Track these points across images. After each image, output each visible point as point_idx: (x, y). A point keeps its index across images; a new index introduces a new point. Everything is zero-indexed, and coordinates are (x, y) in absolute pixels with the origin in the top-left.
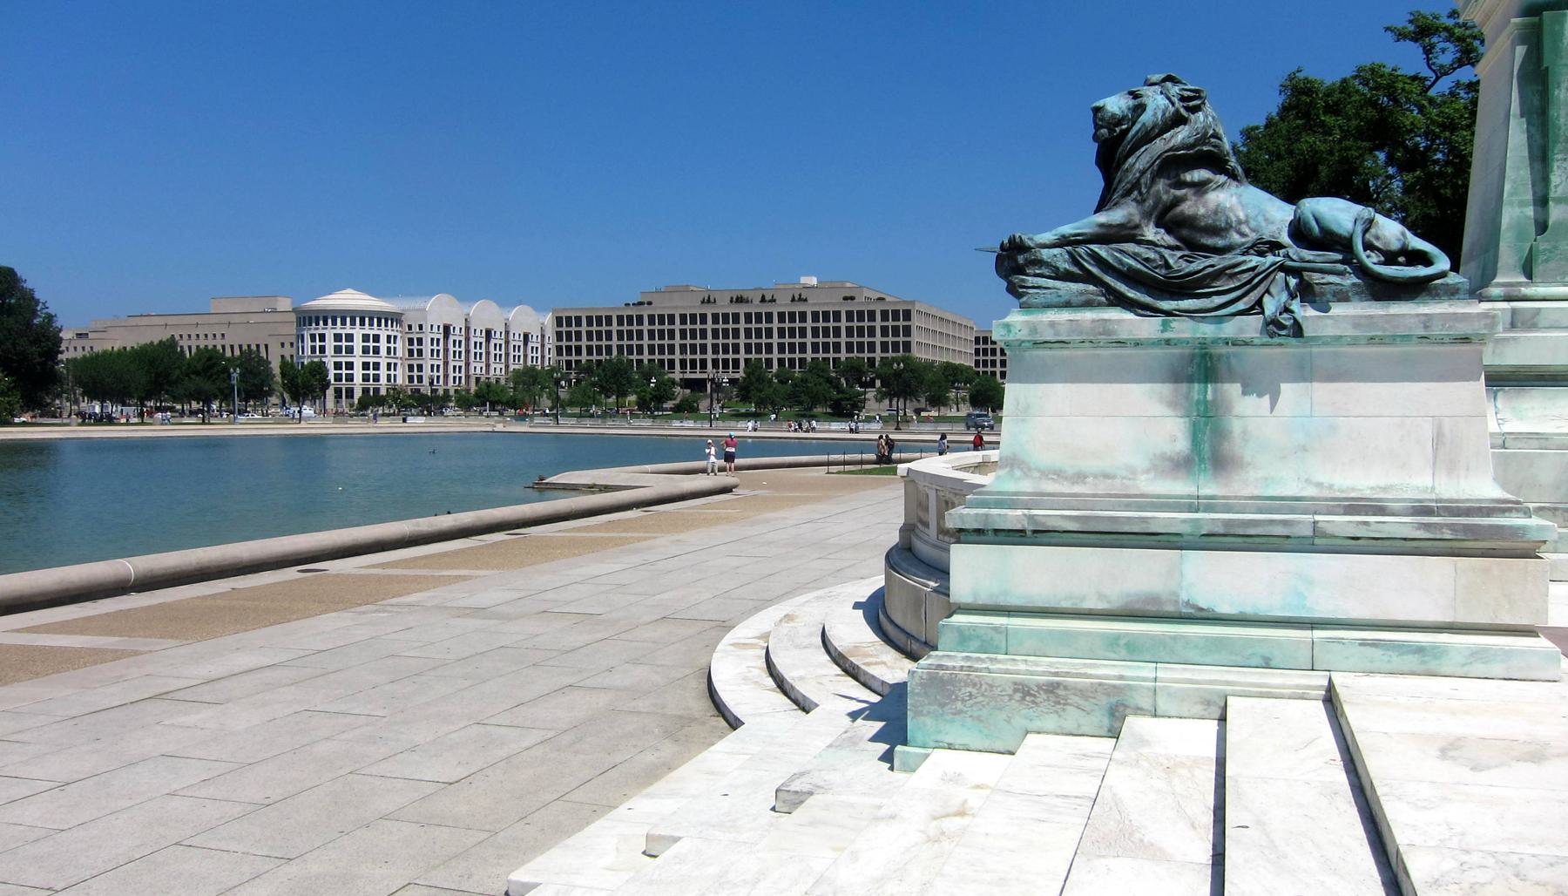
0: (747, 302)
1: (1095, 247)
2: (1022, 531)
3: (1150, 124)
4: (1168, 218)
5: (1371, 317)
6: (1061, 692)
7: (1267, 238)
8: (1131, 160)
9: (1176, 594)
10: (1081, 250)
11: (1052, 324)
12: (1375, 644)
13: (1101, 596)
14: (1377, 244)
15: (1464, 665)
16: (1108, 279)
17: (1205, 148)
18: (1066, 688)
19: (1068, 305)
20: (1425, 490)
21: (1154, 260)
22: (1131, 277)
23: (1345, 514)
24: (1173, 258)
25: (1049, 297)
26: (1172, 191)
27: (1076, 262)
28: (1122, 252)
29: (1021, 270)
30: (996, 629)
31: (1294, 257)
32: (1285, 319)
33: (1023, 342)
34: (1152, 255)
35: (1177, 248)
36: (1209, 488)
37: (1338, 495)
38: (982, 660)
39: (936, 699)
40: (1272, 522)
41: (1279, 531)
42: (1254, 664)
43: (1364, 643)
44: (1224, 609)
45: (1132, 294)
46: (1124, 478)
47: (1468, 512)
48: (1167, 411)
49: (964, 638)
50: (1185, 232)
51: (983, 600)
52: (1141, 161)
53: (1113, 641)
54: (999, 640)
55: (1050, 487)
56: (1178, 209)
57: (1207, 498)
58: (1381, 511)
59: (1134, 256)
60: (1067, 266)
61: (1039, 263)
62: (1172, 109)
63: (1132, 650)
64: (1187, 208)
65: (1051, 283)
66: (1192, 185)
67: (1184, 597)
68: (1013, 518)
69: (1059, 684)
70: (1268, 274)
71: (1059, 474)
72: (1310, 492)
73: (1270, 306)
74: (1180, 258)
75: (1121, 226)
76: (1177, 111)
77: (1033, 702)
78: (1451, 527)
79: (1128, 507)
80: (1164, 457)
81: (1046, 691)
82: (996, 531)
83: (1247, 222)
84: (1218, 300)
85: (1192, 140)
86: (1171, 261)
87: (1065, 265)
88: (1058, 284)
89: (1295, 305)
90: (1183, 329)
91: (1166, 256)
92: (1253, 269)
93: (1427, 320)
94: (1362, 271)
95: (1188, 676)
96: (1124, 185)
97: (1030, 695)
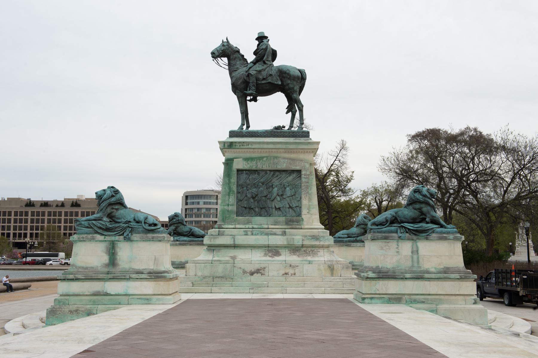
0: (50, 206)
1: (93, 222)
2: (73, 279)
3: (106, 197)
4: (110, 216)
5: (143, 237)
6: (78, 311)
7: (128, 220)
8: (102, 204)
9: (103, 291)
10: (90, 222)
11: (83, 238)
12: (140, 299)
13: (88, 292)
14: (147, 222)
15: (155, 302)
17: (118, 202)
18: (79, 310)
19: (87, 233)
20: (152, 269)
21: (104, 225)
22: (100, 228)
23: (136, 274)
24: (108, 224)
25: (83, 231)
26: (111, 210)
28: (98, 223)
31: (132, 224)
32: (127, 237)
33: (76, 241)
34: (104, 223)
35: (110, 221)
37: (136, 270)
38: (63, 306)
39: (52, 314)
40: (121, 276)
41: (123, 277)
42: (117, 304)
43: (138, 299)
44: (112, 293)
46: (95, 268)
47: (158, 273)
48: (104, 254)
50: (114, 219)
51: (64, 294)
52: (103, 205)
53: (90, 301)
54: (67, 302)
55: (80, 270)
56: (112, 214)
57: (111, 271)
58: (143, 273)
59: (101, 224)
60: (87, 225)
62: (111, 194)
63: (94, 303)
64: (114, 214)
65: (84, 228)
66: (116, 209)
67: (105, 291)
69: (78, 310)
70: (126, 228)
73: (125, 234)
74: (110, 224)
75: (99, 217)
76: (112, 194)
77: (73, 314)
78: (154, 276)
80: (104, 264)
81: (75, 311)
82: (68, 279)
83: (126, 217)
84: (116, 233)
85: (115, 200)
86: (108, 225)
88: (85, 229)
90: (108, 238)
91: (107, 224)
92: (123, 227)
95: (104, 307)
97: (72, 312)
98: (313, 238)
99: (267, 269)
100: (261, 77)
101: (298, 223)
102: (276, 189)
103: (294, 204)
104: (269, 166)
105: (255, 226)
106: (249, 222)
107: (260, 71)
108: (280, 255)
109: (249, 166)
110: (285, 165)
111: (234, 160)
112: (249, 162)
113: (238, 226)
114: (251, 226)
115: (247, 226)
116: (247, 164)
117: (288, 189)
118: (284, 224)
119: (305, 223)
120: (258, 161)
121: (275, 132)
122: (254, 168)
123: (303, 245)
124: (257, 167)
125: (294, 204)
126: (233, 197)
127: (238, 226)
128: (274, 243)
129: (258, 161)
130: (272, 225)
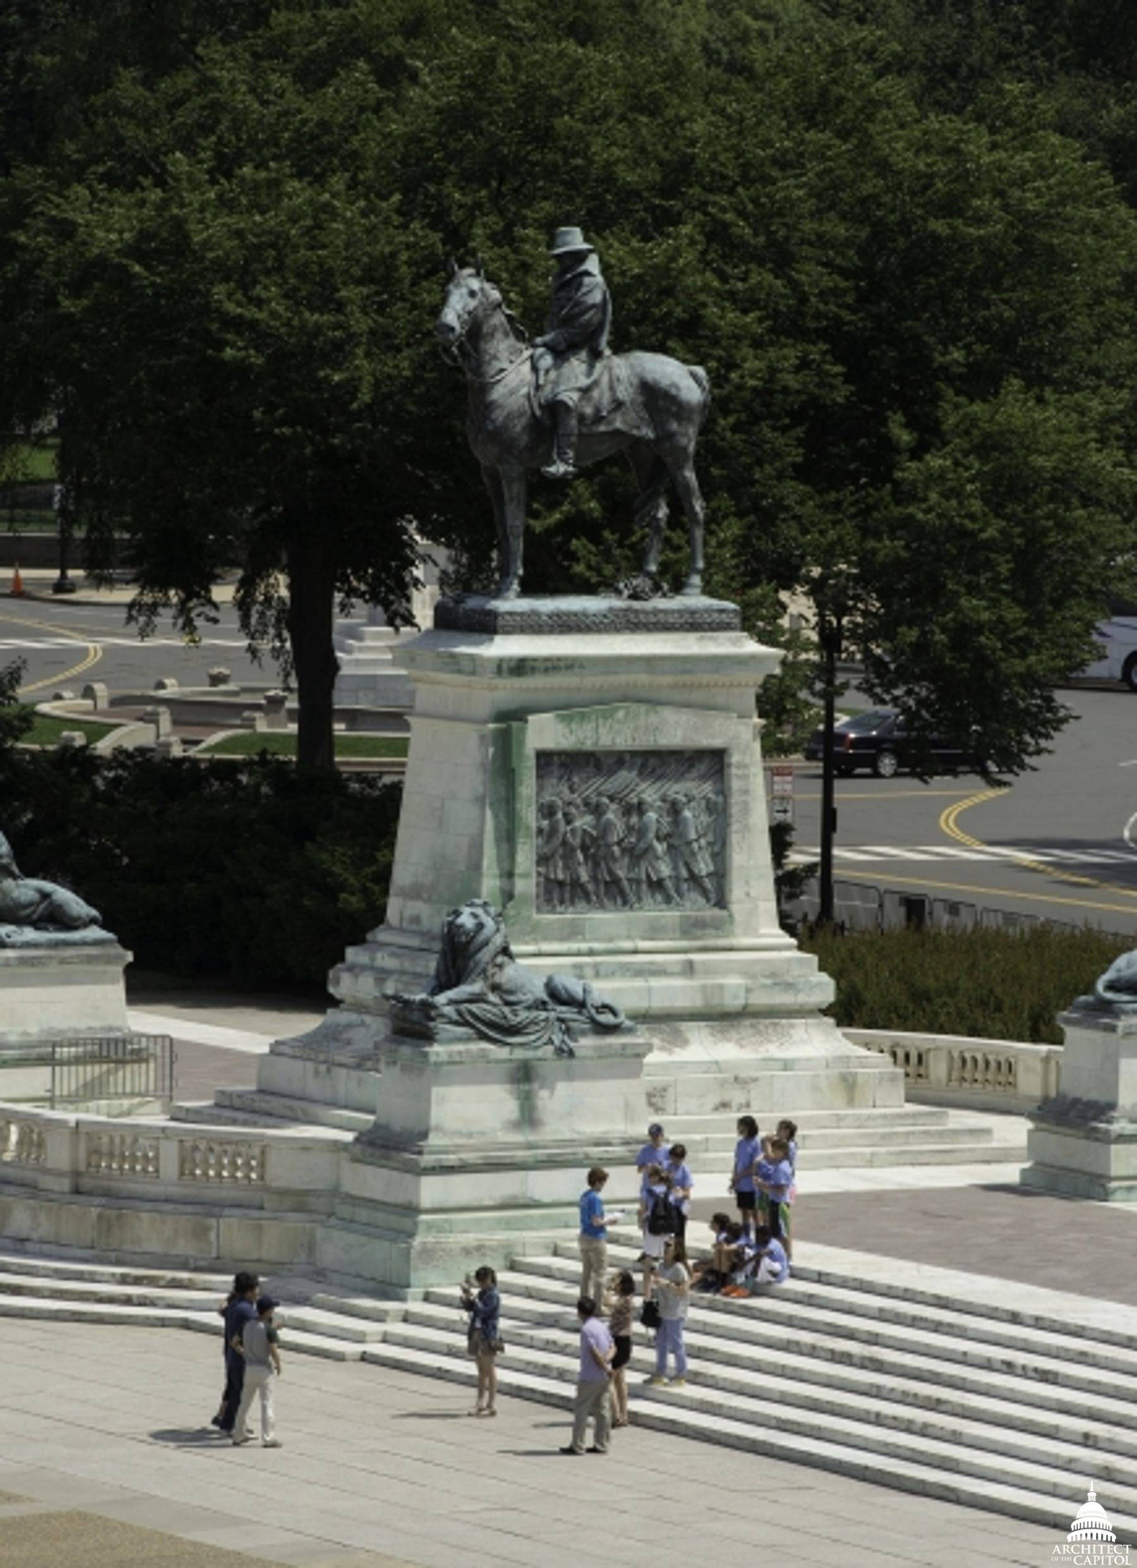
10: (463, 1007)
16: (479, 1026)
22: (492, 1025)
27: (459, 1013)
29: (433, 1019)
30: (446, 1221)
36: (532, 1137)
44: (546, 1199)
45: (491, 1033)
49: (430, 1226)
51: (436, 1205)
53: (499, 1220)
54: (447, 1226)
58: (609, 1144)
61: (442, 1016)
63: (509, 1225)
68: (451, 1159)
71: (459, 1133)
72: (575, 1136)
79: (500, 1150)
84: (533, 1037)
87: (455, 1017)
89: (566, 1038)
93: (624, 1047)
94: (593, 1021)
96: (478, 970)
98: (775, 984)
99: (670, 1094)
100: (588, 410)
101: (716, 928)
102: (652, 815)
103: (702, 865)
104: (634, 739)
105: (596, 946)
106: (573, 932)
107: (585, 391)
108: (685, 1043)
109: (573, 739)
110: (679, 733)
111: (531, 718)
112: (574, 726)
113: (546, 947)
114: (584, 946)
115: (574, 946)
116: (567, 731)
117: (687, 814)
118: (678, 934)
119: (738, 930)
120: (601, 721)
121: (636, 612)
122: (589, 745)
123: (745, 1006)
124: (596, 743)
125: (702, 865)
126: (527, 847)
127: (546, 947)
128: (667, 1004)
129: (601, 721)
130: (644, 939)
